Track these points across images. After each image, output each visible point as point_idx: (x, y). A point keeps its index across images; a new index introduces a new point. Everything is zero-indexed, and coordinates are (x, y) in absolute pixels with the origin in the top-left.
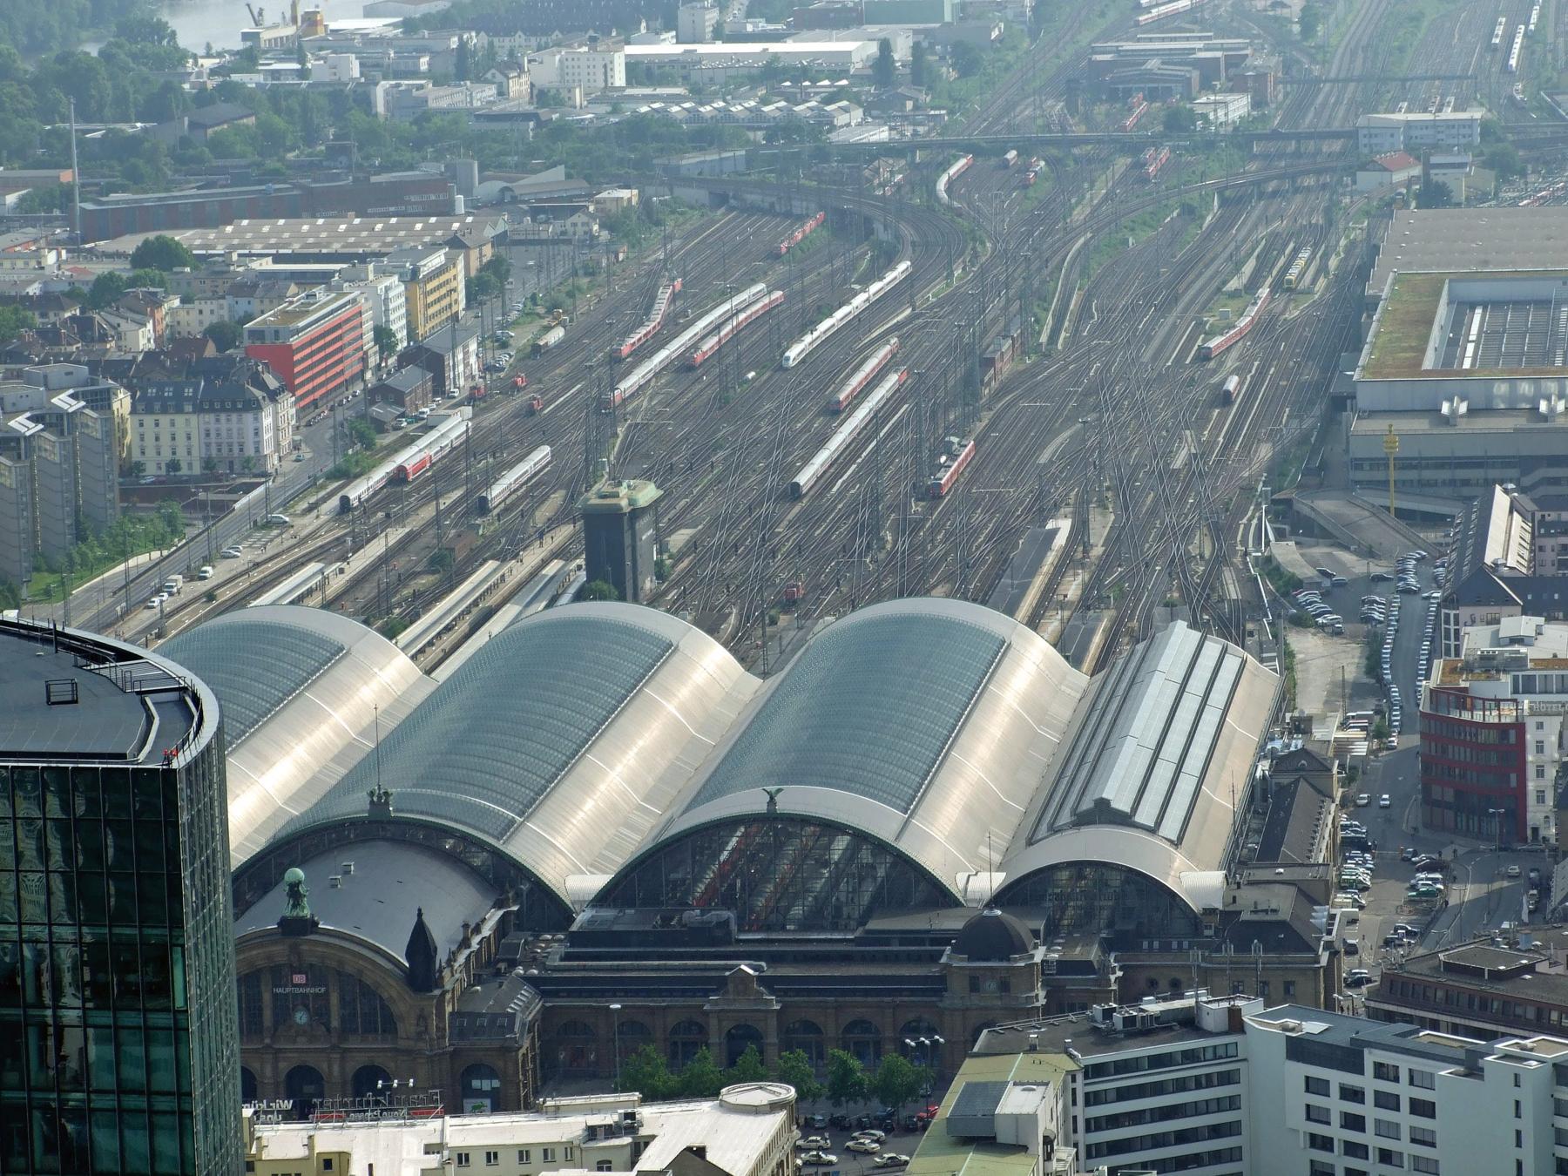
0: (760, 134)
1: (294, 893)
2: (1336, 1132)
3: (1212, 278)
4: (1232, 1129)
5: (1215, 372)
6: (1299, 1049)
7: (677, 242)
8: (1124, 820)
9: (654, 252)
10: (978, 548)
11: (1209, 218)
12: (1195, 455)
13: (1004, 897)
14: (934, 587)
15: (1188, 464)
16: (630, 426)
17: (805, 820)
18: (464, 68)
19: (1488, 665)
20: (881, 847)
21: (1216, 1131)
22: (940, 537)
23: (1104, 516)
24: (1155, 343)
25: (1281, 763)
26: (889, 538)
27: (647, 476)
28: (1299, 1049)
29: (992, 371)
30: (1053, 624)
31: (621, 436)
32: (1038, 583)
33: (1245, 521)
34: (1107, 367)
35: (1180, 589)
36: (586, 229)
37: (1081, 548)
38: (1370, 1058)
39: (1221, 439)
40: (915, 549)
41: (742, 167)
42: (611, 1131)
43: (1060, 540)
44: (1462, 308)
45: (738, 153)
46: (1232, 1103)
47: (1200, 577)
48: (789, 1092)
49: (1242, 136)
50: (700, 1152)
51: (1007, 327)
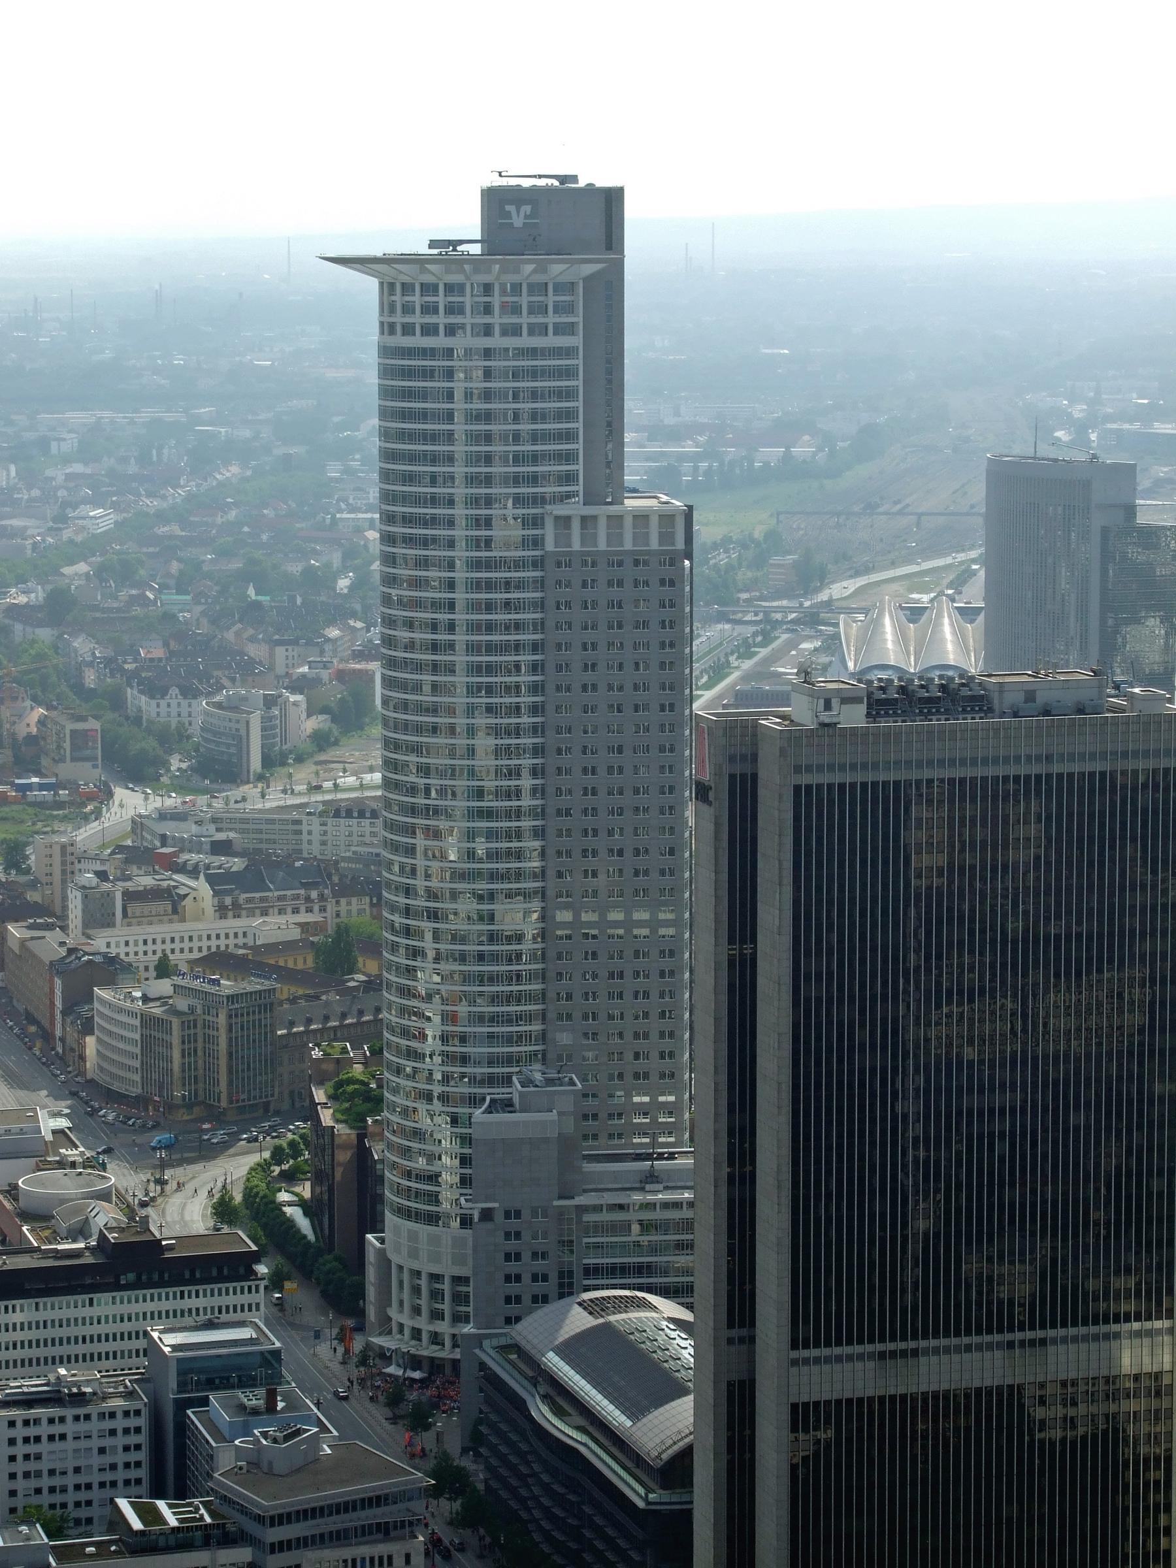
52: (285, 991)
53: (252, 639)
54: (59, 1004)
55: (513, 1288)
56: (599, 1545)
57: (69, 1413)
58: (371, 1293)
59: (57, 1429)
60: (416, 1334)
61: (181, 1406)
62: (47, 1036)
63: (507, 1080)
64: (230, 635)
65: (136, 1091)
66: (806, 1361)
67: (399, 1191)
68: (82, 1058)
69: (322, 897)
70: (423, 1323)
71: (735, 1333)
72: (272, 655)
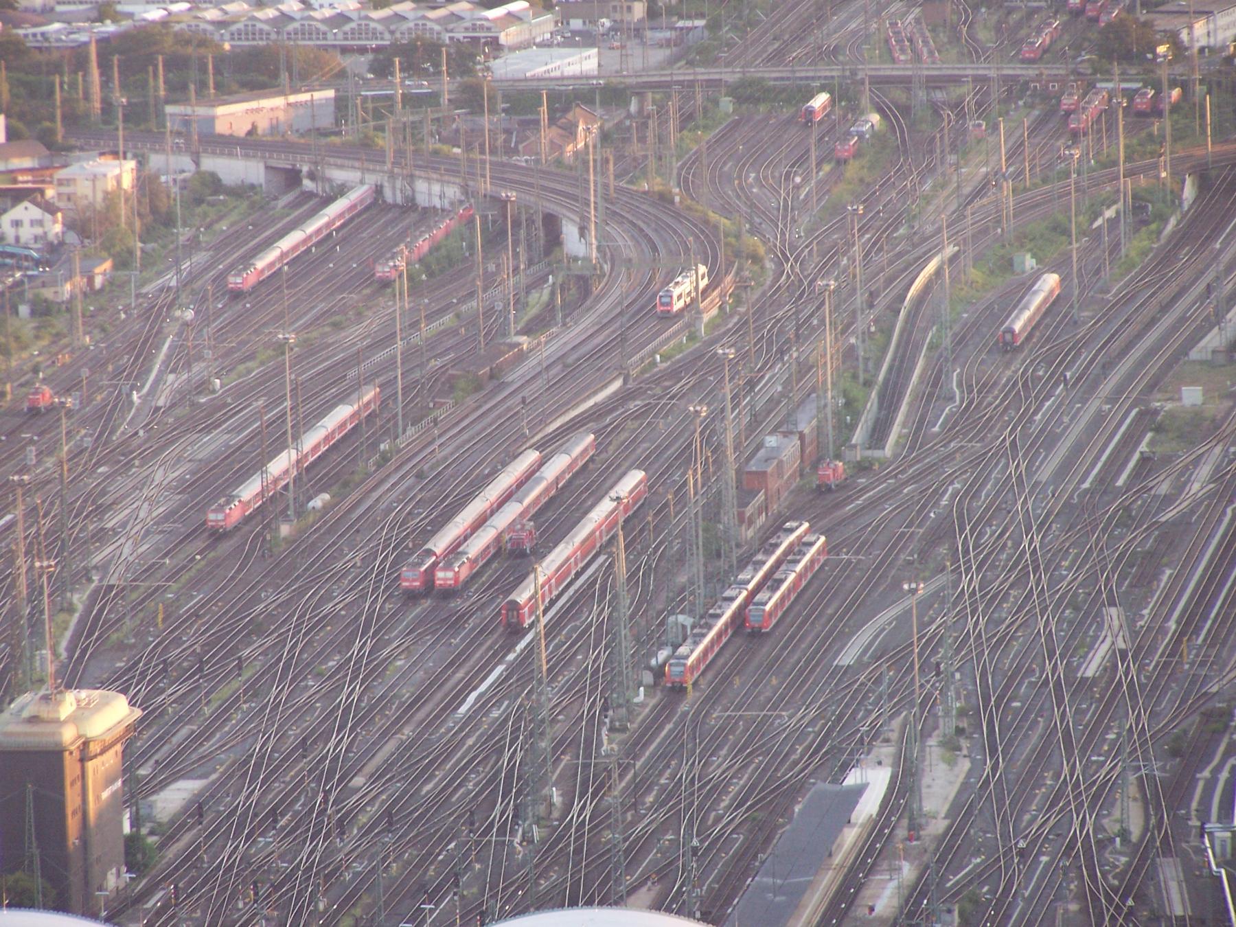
0: (359, 64)
3: (1174, 329)
5: (1168, 500)
7: (200, 258)
9: (160, 274)
10: (718, 819)
11: (1173, 221)
12: (1124, 654)
14: (632, 890)
15: (1110, 669)
16: (96, 591)
22: (650, 799)
23: (952, 763)
24: (1063, 449)
26: (557, 799)
27: (120, 683)
29: (761, 496)
31: (80, 607)
32: (825, 883)
33: (1206, 773)
34: (972, 492)
35: (1081, 896)
36: (38, 231)
37: (905, 822)
39: (1172, 625)
40: (600, 819)
41: (326, 121)
43: (868, 807)
45: (318, 95)
47: (1120, 876)
51: (789, 418)
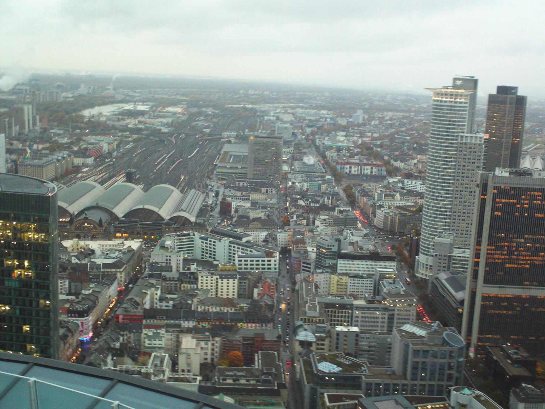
1: (86, 214)
2: (204, 247)
4: (193, 247)
6: (201, 238)
8: (185, 211)
13: (171, 219)
17: (147, 209)
18: (119, 120)
19: (229, 196)
20: (157, 214)
21: (191, 247)
25: (204, 206)
28: (201, 238)
30: (180, 189)
38: (209, 239)
42: (120, 243)
44: (231, 156)
46: (193, 244)
48: (142, 240)
49: (210, 134)
50: (130, 246)
52: (409, 214)
53: (414, 154)
54: (371, 212)
55: (439, 268)
56: (448, 313)
57: (360, 279)
58: (416, 266)
59: (363, 282)
60: (423, 274)
61: (379, 281)
62: (369, 217)
63: (442, 233)
64: (410, 153)
65: (382, 228)
66: (486, 287)
67: (422, 249)
68: (374, 221)
69: (419, 199)
70: (423, 272)
71: (474, 280)
72: (417, 156)
